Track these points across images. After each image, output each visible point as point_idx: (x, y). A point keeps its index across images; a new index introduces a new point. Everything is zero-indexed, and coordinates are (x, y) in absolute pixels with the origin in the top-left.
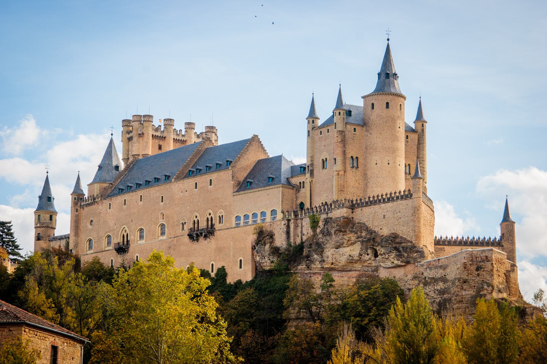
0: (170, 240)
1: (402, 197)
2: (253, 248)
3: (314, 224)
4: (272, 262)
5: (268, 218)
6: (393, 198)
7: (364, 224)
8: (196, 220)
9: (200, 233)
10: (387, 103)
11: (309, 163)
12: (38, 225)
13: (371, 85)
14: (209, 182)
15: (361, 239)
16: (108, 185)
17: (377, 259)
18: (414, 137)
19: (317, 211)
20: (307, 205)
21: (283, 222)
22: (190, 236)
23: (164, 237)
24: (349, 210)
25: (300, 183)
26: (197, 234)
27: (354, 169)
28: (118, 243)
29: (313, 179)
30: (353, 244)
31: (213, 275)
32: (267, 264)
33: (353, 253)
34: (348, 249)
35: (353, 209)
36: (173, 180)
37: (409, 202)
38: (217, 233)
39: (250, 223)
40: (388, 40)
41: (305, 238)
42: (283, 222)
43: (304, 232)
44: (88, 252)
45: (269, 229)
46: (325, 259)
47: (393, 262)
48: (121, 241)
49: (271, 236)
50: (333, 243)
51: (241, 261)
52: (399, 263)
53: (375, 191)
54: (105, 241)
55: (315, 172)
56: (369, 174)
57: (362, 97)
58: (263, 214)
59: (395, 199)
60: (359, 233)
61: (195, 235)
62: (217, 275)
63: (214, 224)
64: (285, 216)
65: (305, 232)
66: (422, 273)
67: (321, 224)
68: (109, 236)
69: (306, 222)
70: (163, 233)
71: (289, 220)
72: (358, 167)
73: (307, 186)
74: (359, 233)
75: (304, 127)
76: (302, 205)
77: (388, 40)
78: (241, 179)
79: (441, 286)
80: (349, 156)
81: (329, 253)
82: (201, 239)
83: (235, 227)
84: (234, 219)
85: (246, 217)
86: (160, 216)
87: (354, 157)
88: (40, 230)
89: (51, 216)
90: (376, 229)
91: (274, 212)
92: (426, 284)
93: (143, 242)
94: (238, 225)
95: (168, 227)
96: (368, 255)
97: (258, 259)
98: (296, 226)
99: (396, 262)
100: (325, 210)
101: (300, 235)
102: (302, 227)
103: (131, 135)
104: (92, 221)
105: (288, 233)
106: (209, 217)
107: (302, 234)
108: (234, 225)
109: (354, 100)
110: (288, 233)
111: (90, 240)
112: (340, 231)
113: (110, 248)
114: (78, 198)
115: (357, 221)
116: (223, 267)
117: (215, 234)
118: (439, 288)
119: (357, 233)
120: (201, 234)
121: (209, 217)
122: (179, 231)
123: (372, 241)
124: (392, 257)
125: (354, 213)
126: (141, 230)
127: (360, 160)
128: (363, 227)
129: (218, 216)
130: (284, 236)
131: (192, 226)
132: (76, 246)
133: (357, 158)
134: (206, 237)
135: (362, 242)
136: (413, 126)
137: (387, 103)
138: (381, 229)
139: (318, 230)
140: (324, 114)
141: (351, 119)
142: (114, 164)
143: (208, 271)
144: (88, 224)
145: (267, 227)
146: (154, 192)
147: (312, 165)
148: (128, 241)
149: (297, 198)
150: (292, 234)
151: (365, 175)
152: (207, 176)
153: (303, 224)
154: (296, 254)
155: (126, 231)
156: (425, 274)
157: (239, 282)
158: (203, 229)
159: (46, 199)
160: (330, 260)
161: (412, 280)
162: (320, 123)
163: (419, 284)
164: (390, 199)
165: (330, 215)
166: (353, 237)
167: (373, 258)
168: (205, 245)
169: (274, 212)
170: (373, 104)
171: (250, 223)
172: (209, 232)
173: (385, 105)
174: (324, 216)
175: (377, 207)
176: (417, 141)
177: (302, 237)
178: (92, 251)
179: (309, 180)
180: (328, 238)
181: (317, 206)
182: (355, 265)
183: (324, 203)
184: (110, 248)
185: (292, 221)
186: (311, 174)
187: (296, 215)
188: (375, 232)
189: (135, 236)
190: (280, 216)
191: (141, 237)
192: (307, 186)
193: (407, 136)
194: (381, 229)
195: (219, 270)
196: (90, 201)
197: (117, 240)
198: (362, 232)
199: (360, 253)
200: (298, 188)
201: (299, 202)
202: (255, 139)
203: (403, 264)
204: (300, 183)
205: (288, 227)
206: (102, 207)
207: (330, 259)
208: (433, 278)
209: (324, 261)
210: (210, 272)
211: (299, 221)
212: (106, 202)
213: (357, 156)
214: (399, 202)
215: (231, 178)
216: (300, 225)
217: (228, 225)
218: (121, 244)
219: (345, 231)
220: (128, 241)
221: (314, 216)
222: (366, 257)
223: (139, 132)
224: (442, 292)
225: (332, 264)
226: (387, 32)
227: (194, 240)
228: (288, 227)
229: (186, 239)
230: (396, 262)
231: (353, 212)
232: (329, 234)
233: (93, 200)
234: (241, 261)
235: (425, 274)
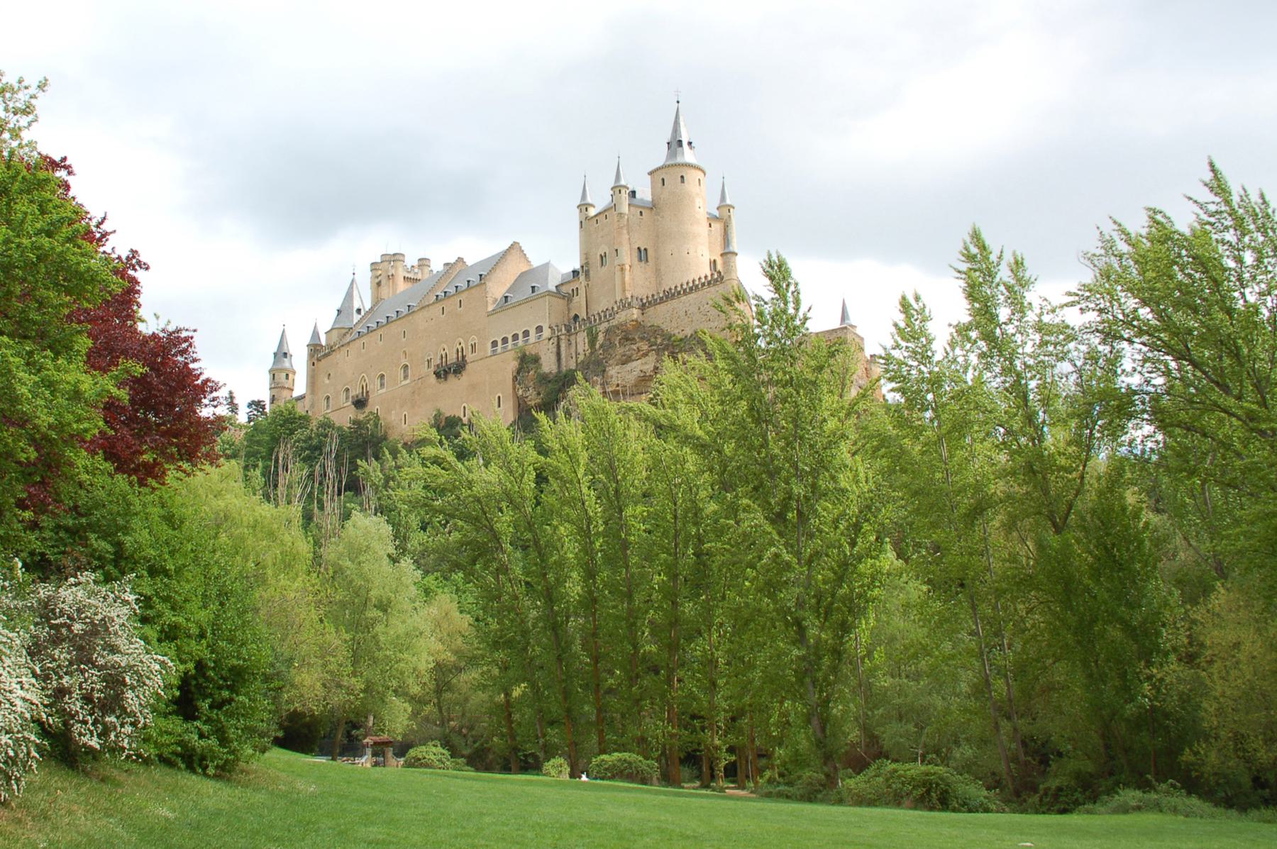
1: (709, 283)
2: (515, 379)
4: (539, 394)
5: (532, 337)
9: (450, 370)
18: (717, 226)
20: (583, 315)
22: (437, 375)
27: (643, 264)
30: (646, 355)
33: (645, 368)
41: (581, 358)
49: (536, 360)
54: (343, 396)
55: (591, 273)
56: (662, 268)
57: (650, 173)
58: (526, 333)
65: (580, 350)
67: (601, 337)
68: (347, 390)
69: (582, 340)
70: (406, 377)
73: (582, 292)
75: (575, 217)
76: (576, 317)
81: (613, 371)
82: (451, 377)
84: (489, 345)
85: (505, 340)
86: (402, 356)
88: (275, 392)
91: (539, 329)
93: (384, 390)
94: (494, 353)
97: (520, 392)
105: (558, 354)
107: (577, 354)
110: (558, 354)
111: (328, 398)
112: (627, 339)
114: (317, 352)
128: (656, 331)
130: (554, 358)
132: (312, 406)
136: (717, 213)
139: (597, 346)
140: (600, 200)
141: (634, 201)
142: (357, 305)
145: (531, 350)
146: (395, 329)
147: (587, 264)
149: (569, 310)
151: (658, 272)
159: (282, 354)
164: (694, 288)
169: (539, 329)
172: (459, 367)
174: (606, 325)
187: (568, 331)
190: (547, 333)
191: (382, 385)
192: (582, 292)
197: (356, 392)
200: (569, 298)
201: (572, 315)
202: (515, 246)
205: (559, 347)
206: (337, 357)
211: (573, 338)
212: (344, 349)
214: (706, 289)
217: (482, 354)
228: (559, 347)
233: (331, 350)
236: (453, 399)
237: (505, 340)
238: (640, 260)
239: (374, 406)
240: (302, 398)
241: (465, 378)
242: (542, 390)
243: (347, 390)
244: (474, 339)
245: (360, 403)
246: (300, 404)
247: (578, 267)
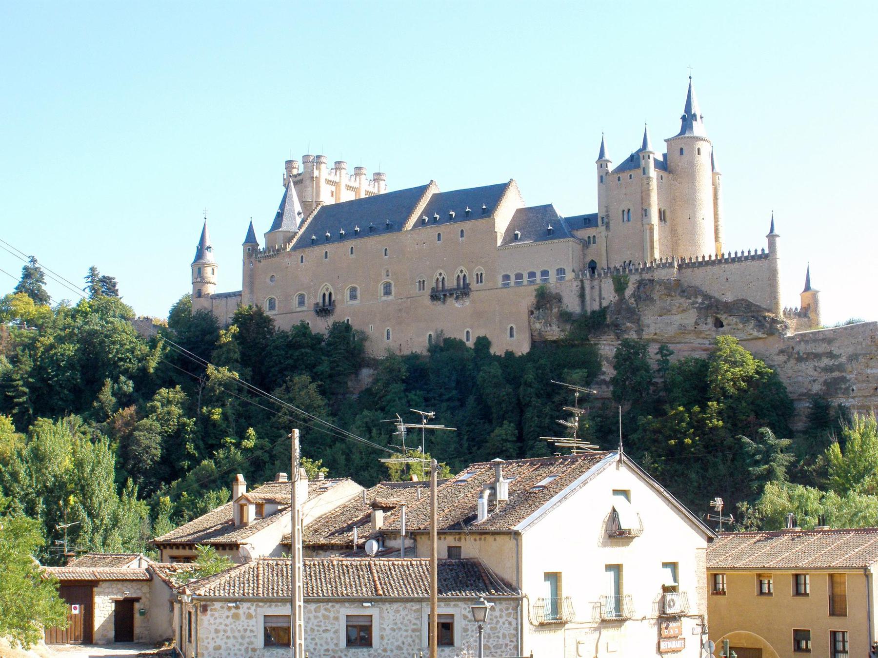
0: (400, 301)
3: (620, 287)
11: (603, 214)
12: (199, 280)
21: (575, 284)
23: (390, 298)
25: (589, 237)
30: (684, 311)
31: (470, 344)
32: (555, 332)
33: (686, 322)
34: (678, 317)
37: (764, 263)
39: (525, 283)
41: (605, 304)
42: (575, 284)
43: (603, 296)
45: (554, 291)
51: (511, 328)
52: (761, 335)
54: (296, 301)
55: (612, 225)
58: (545, 273)
60: (693, 299)
61: (438, 295)
63: (469, 284)
64: (577, 277)
65: (604, 294)
66: (793, 348)
71: (582, 281)
74: (693, 299)
79: (826, 362)
82: (451, 301)
85: (519, 276)
91: (561, 271)
92: (800, 359)
94: (506, 286)
95: (395, 286)
97: (538, 326)
98: (592, 288)
99: (756, 333)
101: (597, 299)
102: (600, 290)
104: (272, 276)
105: (582, 296)
106: (461, 276)
107: (601, 298)
108: (500, 285)
110: (582, 296)
113: (304, 308)
117: (471, 294)
118: (822, 365)
119: (690, 299)
122: (415, 290)
123: (714, 308)
124: (751, 327)
128: (696, 291)
131: (434, 285)
134: (457, 298)
135: (699, 309)
144: (268, 280)
146: (374, 243)
149: (584, 255)
150: (588, 297)
153: (603, 285)
154: (595, 322)
155: (327, 289)
156: (797, 349)
157: (510, 355)
158: (451, 290)
160: (652, 329)
161: (778, 354)
163: (789, 360)
166: (685, 302)
167: (714, 329)
169: (561, 271)
171: (525, 283)
180: (647, 302)
182: (687, 336)
183: (627, 262)
184: (304, 308)
189: (343, 295)
190: (569, 275)
191: (353, 297)
195: (479, 338)
196: (271, 253)
198: (696, 297)
200: (586, 244)
203: (765, 336)
204: (589, 237)
208: (812, 353)
210: (465, 340)
211: (596, 283)
214: (749, 263)
216: (597, 287)
218: (321, 304)
224: (828, 369)
225: (655, 334)
228: (583, 288)
229: (427, 301)
230: (756, 333)
234: (511, 328)
235: (797, 349)
237: (519, 276)
241: (467, 302)
242: (568, 327)
244: (479, 269)
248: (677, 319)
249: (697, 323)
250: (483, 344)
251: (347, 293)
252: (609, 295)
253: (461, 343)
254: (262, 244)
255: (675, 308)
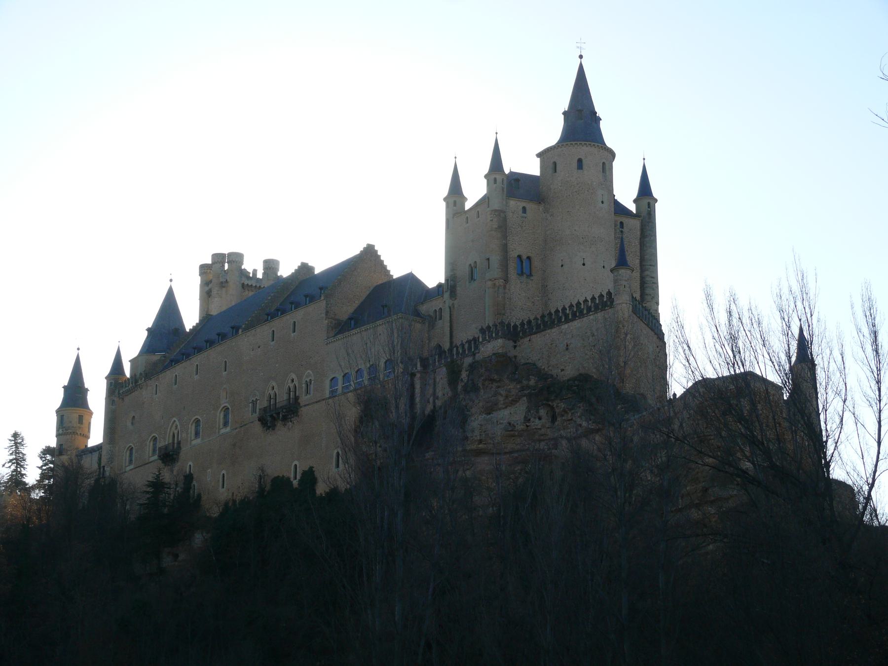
4: (385, 450)
6: (581, 312)
7: (534, 364)
8: (272, 393)
10: (580, 161)
13: (552, 132)
14: (292, 327)
15: (526, 392)
16: (158, 357)
17: (556, 423)
19: (458, 353)
20: (446, 346)
22: (262, 420)
23: (228, 429)
24: (507, 342)
26: (272, 416)
27: (524, 278)
28: (166, 447)
29: (456, 302)
30: (514, 402)
31: (295, 483)
35: (515, 342)
36: (240, 331)
38: (303, 411)
40: (581, 57)
41: (439, 403)
44: (128, 469)
46: (469, 435)
47: (580, 425)
48: (171, 441)
50: (481, 404)
53: (556, 304)
55: (458, 288)
57: (539, 155)
59: (585, 312)
60: (525, 382)
62: (301, 481)
65: (440, 394)
67: (464, 375)
68: (155, 439)
69: (442, 374)
70: (226, 424)
72: (530, 275)
76: (439, 346)
77: (581, 57)
78: (344, 317)
80: (514, 254)
81: (476, 421)
82: (279, 424)
83: (329, 398)
87: (524, 257)
89: (81, 418)
90: (554, 372)
93: (199, 441)
96: (540, 419)
100: (470, 348)
101: (431, 400)
103: (210, 286)
106: (292, 386)
108: (327, 395)
109: (524, 162)
112: (493, 381)
115: (523, 361)
116: (311, 468)
119: (520, 382)
120: (278, 414)
121: (292, 386)
125: (518, 348)
126: (197, 422)
127: (536, 263)
128: (532, 368)
129: (304, 382)
132: (111, 460)
133: (529, 258)
134: (285, 419)
136: (632, 208)
137: (580, 161)
138: (562, 370)
139: (460, 387)
140: (475, 190)
143: (289, 479)
144: (129, 424)
148: (179, 443)
150: (417, 400)
152: (288, 317)
155: (176, 427)
159: (75, 393)
162: (468, 205)
164: (577, 312)
165: (479, 357)
168: (286, 436)
170: (555, 164)
173: (575, 164)
174: (468, 361)
175: (555, 331)
176: (639, 233)
177: (434, 402)
178: (132, 467)
179: (449, 302)
181: (459, 344)
185: (418, 375)
186: (451, 292)
188: (552, 376)
189: (187, 434)
191: (197, 434)
193: (622, 223)
194: (562, 370)
195: (304, 473)
198: (529, 380)
199: (525, 417)
201: (433, 344)
207: (477, 433)
209: (466, 438)
213: (530, 255)
215: (324, 315)
216: (431, 382)
218: (171, 448)
219: (500, 381)
220: (179, 443)
221: (452, 361)
222: (536, 423)
223: (221, 280)
225: (480, 441)
226: (579, 45)
227: (269, 428)
228: (412, 386)
229: (257, 427)
230: (584, 424)
231: (515, 347)
232: (475, 389)
234: (338, 453)
236: (284, 455)
238: (521, 274)
239: (187, 463)
240: (98, 448)
243: (155, 439)
245: (169, 456)
246: (96, 456)
247: (443, 281)
248: (504, 415)
249: (527, 420)
250: (309, 477)
251: (192, 429)
252: (443, 390)
253: (288, 481)
254: (128, 373)
255: (501, 399)
